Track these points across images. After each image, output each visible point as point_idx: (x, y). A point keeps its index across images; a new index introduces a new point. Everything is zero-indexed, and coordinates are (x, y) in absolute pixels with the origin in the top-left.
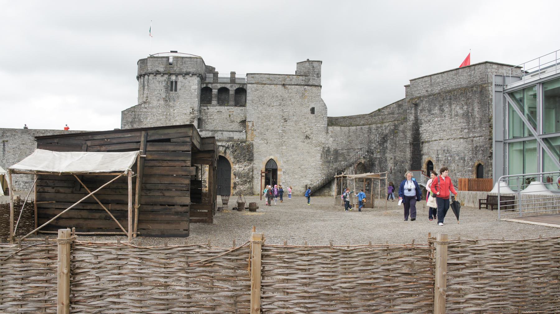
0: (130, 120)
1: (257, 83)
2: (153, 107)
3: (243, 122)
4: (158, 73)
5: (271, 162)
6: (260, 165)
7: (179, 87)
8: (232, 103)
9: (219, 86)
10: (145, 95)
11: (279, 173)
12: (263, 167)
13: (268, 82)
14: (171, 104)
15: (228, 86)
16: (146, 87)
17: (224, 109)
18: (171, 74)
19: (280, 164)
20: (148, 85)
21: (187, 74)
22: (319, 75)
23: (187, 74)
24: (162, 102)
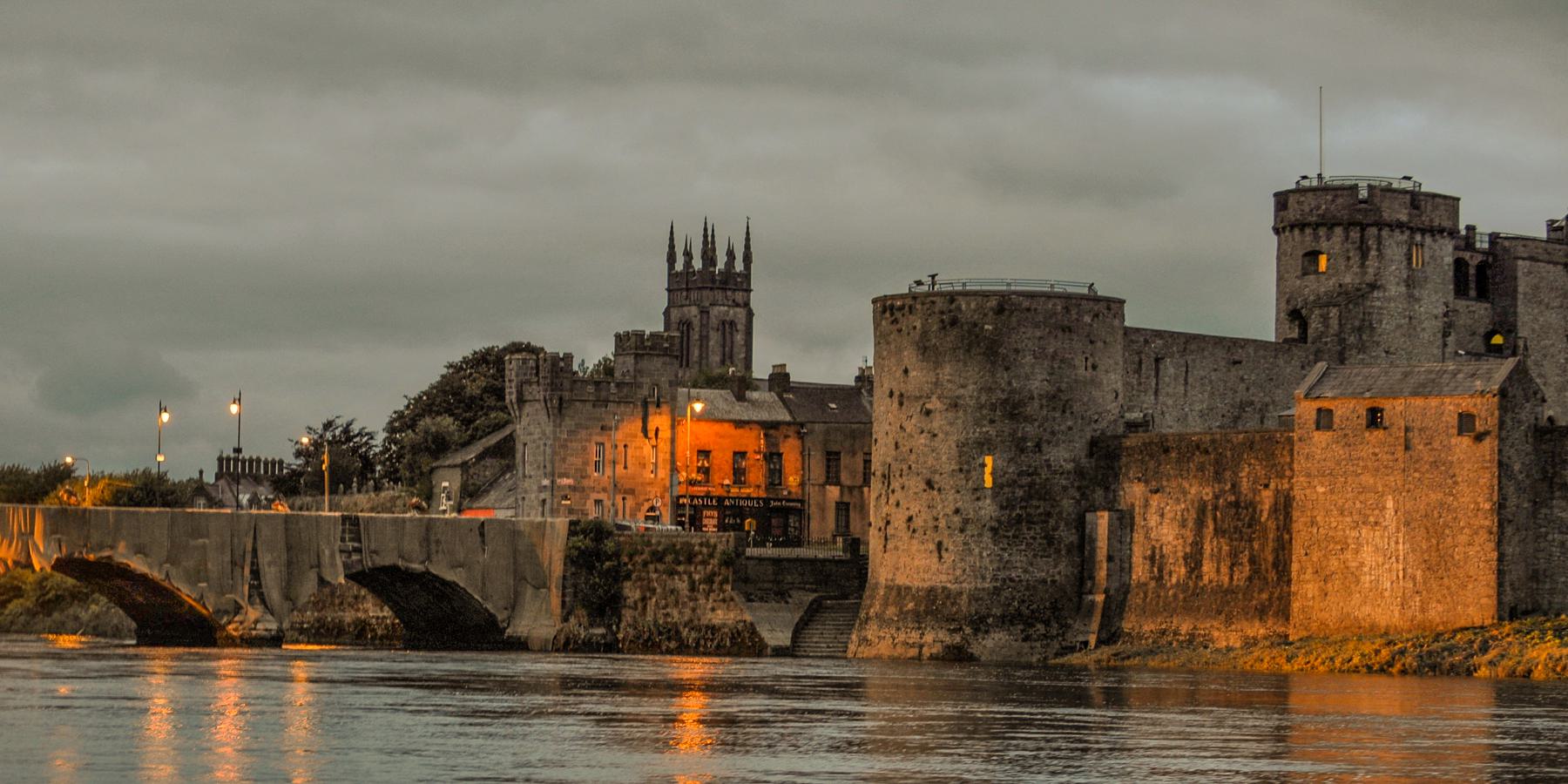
0: (1357, 323)
1: (1531, 259)
2: (1389, 300)
8: (1473, 293)
10: (1371, 270)
13: (1546, 257)
14: (1416, 293)
15: (1467, 255)
16: (1373, 253)
17: (1461, 304)
20: (1378, 250)
21: (1441, 231)
23: (1441, 231)
24: (1403, 289)
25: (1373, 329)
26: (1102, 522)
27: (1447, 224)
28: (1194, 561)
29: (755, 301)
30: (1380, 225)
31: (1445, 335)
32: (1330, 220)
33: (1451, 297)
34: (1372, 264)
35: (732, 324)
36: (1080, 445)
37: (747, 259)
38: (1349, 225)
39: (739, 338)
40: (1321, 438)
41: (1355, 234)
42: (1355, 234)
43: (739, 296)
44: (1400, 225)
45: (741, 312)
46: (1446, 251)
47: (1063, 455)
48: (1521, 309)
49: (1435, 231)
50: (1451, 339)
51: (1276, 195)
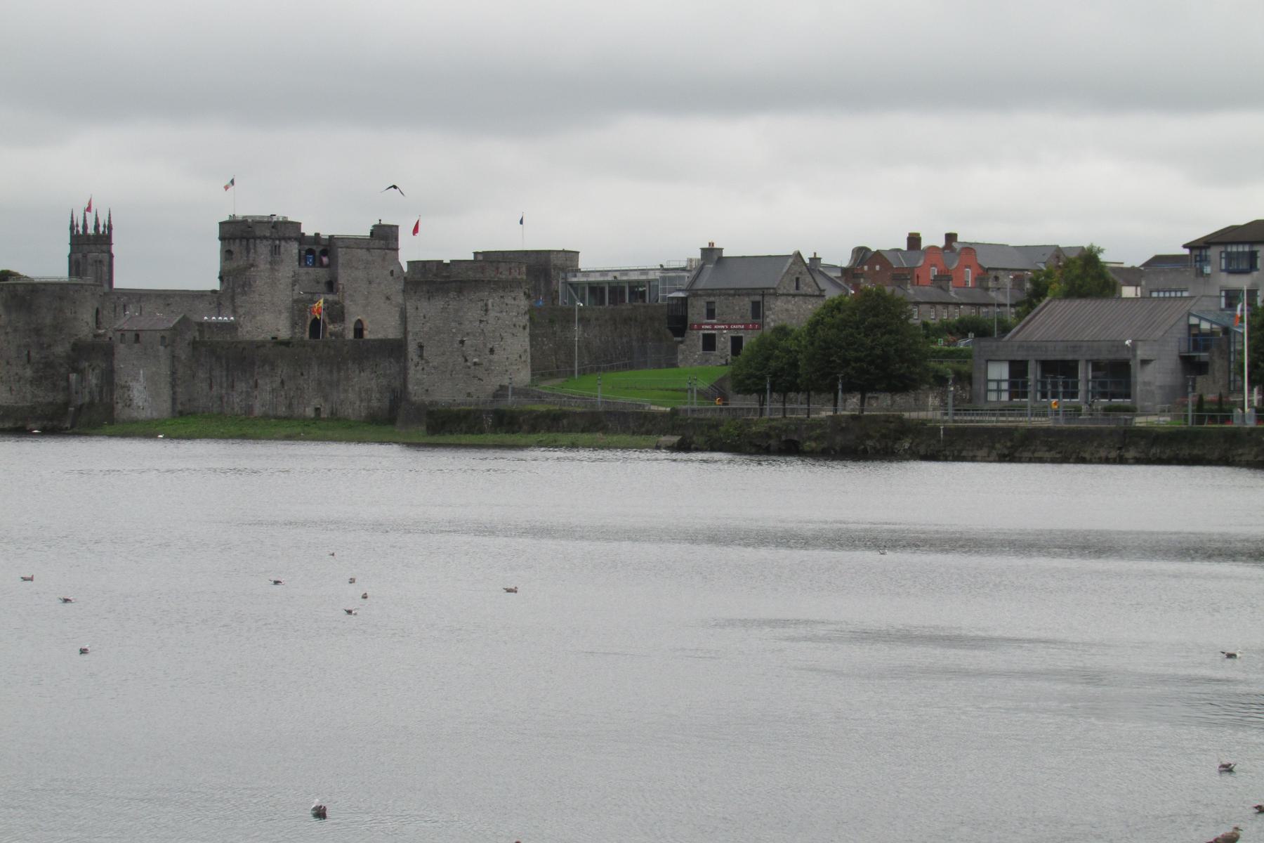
3: (331, 286)
4: (265, 238)
5: (359, 321)
6: (350, 326)
7: (282, 249)
9: (307, 247)
11: (365, 332)
12: (352, 326)
15: (314, 247)
18: (274, 240)
19: (366, 324)
22: (397, 239)
23: (290, 239)
25: (250, 285)
26: (73, 377)
27: (293, 235)
28: (101, 392)
29: (114, 249)
30: (255, 238)
31: (293, 285)
32: (240, 236)
33: (297, 268)
34: (252, 255)
35: (101, 262)
36: (68, 347)
37: (110, 228)
38: (241, 238)
39: (105, 269)
40: (122, 346)
41: (244, 243)
42: (244, 243)
43: (105, 248)
44: (265, 238)
45: (106, 255)
46: (294, 248)
47: (61, 349)
48: (340, 271)
49: (287, 239)
50: (296, 287)
51: (221, 224)
